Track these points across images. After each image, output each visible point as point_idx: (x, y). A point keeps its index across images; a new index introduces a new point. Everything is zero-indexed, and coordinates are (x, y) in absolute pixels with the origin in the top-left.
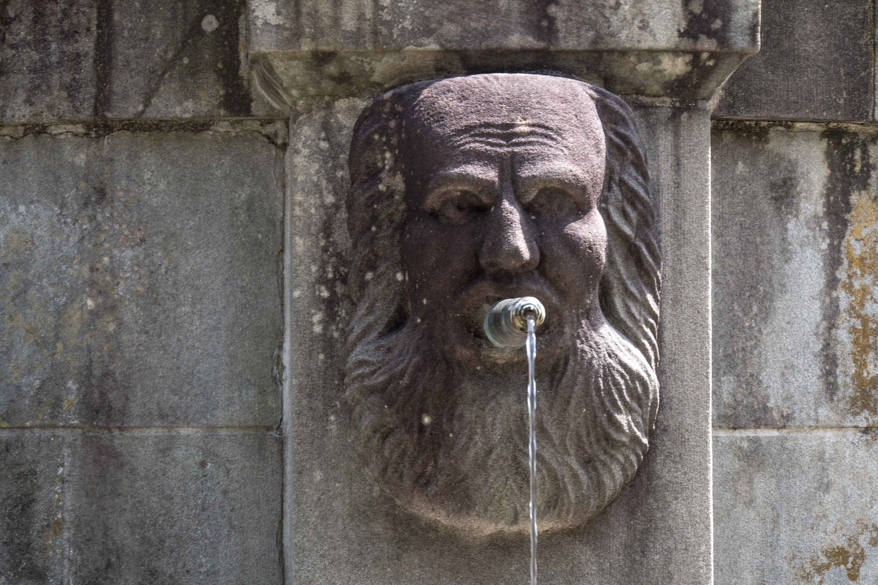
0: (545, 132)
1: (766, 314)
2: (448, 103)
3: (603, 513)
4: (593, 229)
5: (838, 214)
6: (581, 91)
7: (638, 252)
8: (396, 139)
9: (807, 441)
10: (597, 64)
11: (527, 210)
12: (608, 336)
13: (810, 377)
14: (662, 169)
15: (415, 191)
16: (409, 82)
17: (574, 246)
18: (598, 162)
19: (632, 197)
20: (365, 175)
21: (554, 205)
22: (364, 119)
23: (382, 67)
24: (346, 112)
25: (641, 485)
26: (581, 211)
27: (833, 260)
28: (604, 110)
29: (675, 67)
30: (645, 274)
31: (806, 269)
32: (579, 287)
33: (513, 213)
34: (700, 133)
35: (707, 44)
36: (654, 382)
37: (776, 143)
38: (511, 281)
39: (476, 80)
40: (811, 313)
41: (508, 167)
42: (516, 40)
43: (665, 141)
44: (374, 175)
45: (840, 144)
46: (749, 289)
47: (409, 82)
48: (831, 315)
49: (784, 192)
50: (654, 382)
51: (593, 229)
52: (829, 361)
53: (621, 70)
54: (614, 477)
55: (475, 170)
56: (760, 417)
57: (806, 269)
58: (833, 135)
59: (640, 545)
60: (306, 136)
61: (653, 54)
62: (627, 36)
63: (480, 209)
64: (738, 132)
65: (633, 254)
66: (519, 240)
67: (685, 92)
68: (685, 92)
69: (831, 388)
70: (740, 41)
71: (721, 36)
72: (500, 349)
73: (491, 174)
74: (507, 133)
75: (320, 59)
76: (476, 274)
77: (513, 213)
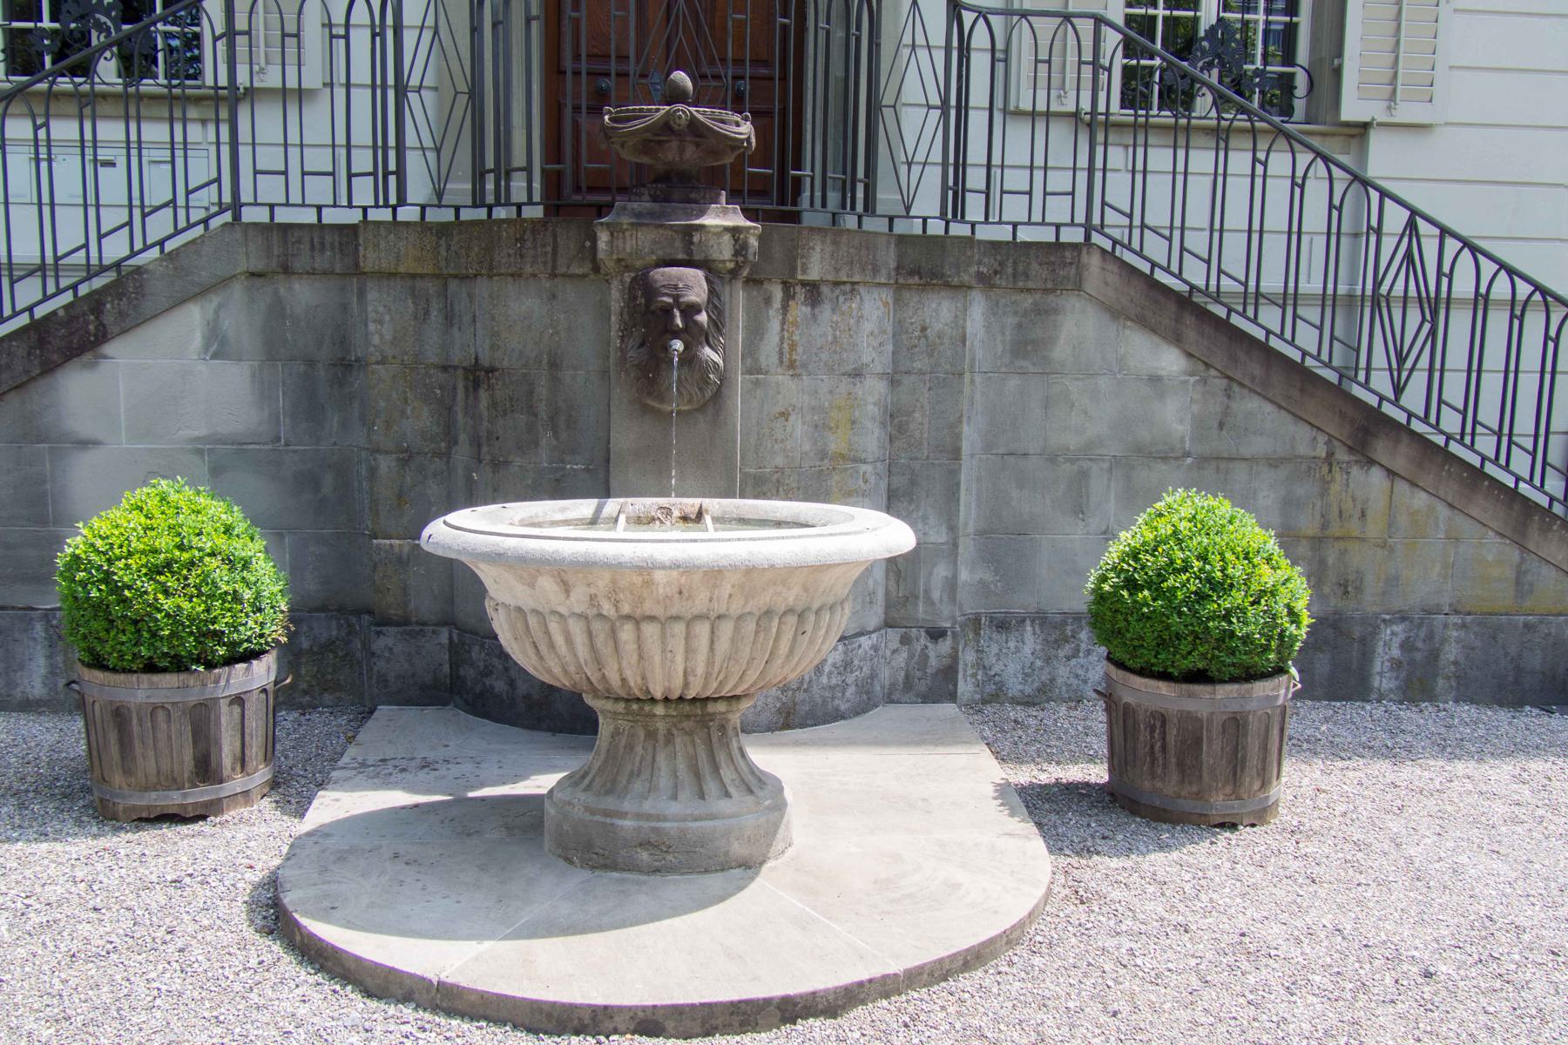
0: (687, 287)
1: (762, 339)
2: (658, 277)
3: (705, 404)
4: (703, 318)
5: (785, 308)
6: (699, 274)
7: (717, 324)
8: (642, 287)
9: (772, 379)
10: (705, 265)
11: (682, 312)
12: (707, 351)
13: (774, 359)
14: (726, 297)
15: (648, 305)
16: (648, 268)
17: (696, 323)
18: (705, 296)
19: (716, 307)
20: (633, 298)
21: (690, 310)
22: (634, 280)
23: (638, 264)
24: (628, 277)
25: (718, 395)
26: (699, 312)
27: (783, 323)
28: (707, 279)
29: (731, 265)
30: (719, 331)
31: (774, 325)
32: (694, 335)
33: (677, 312)
34: (739, 285)
35: (741, 259)
36: (721, 363)
37: (766, 285)
38: (676, 334)
39: (667, 269)
40: (776, 339)
41: (676, 298)
42: (680, 256)
43: (727, 289)
44: (635, 298)
45: (786, 286)
46: (756, 331)
47: (648, 268)
48: (782, 340)
49: (768, 301)
50: (721, 363)
51: (703, 318)
52: (781, 353)
53: (714, 266)
54: (708, 394)
55: (666, 299)
56: (759, 371)
57: (774, 325)
58: (784, 283)
59: (717, 414)
60: (615, 283)
61: (724, 262)
62: (715, 256)
63: (667, 311)
64: (753, 282)
65: (716, 325)
66: (679, 322)
67: (734, 273)
68: (734, 273)
69: (781, 362)
70: (751, 258)
71: (745, 256)
72: (406, 550)
73: (670, 300)
74: (676, 287)
75: (619, 260)
76: (666, 331)
77: (677, 312)
